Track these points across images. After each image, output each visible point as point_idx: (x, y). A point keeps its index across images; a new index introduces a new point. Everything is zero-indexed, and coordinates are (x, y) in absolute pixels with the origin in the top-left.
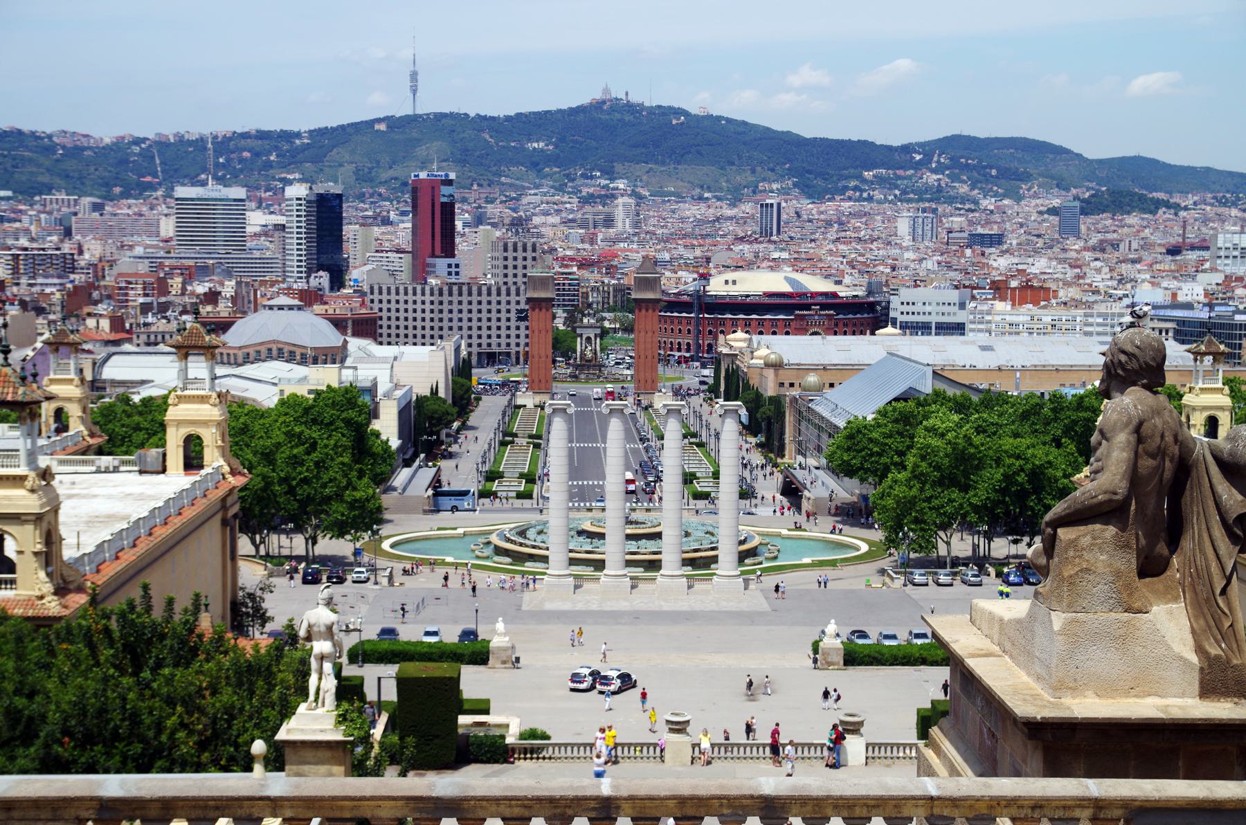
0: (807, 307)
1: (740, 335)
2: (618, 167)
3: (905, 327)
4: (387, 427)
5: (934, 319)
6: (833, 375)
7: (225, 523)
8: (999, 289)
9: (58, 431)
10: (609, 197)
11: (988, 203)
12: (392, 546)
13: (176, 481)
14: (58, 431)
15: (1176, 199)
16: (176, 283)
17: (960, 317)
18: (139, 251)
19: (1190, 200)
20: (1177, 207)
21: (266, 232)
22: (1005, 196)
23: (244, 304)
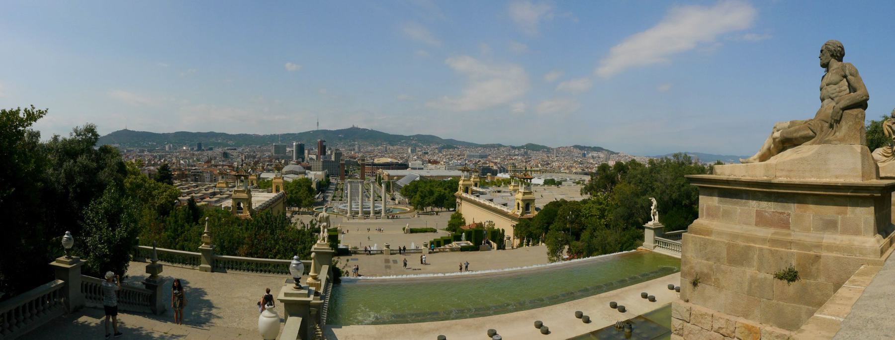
0: (393, 165)
1: (381, 170)
2: (356, 140)
3: (412, 169)
4: (314, 186)
5: (417, 167)
6: (399, 177)
7: (284, 203)
8: (430, 162)
9: (252, 185)
10: (354, 145)
11: (424, 146)
12: (315, 209)
13: (273, 195)
14: (252, 185)
15: (458, 147)
16: (273, 161)
17: (423, 167)
18: (267, 155)
19: (461, 147)
20: (458, 148)
21: (290, 152)
22: (428, 145)
23: (286, 164)
